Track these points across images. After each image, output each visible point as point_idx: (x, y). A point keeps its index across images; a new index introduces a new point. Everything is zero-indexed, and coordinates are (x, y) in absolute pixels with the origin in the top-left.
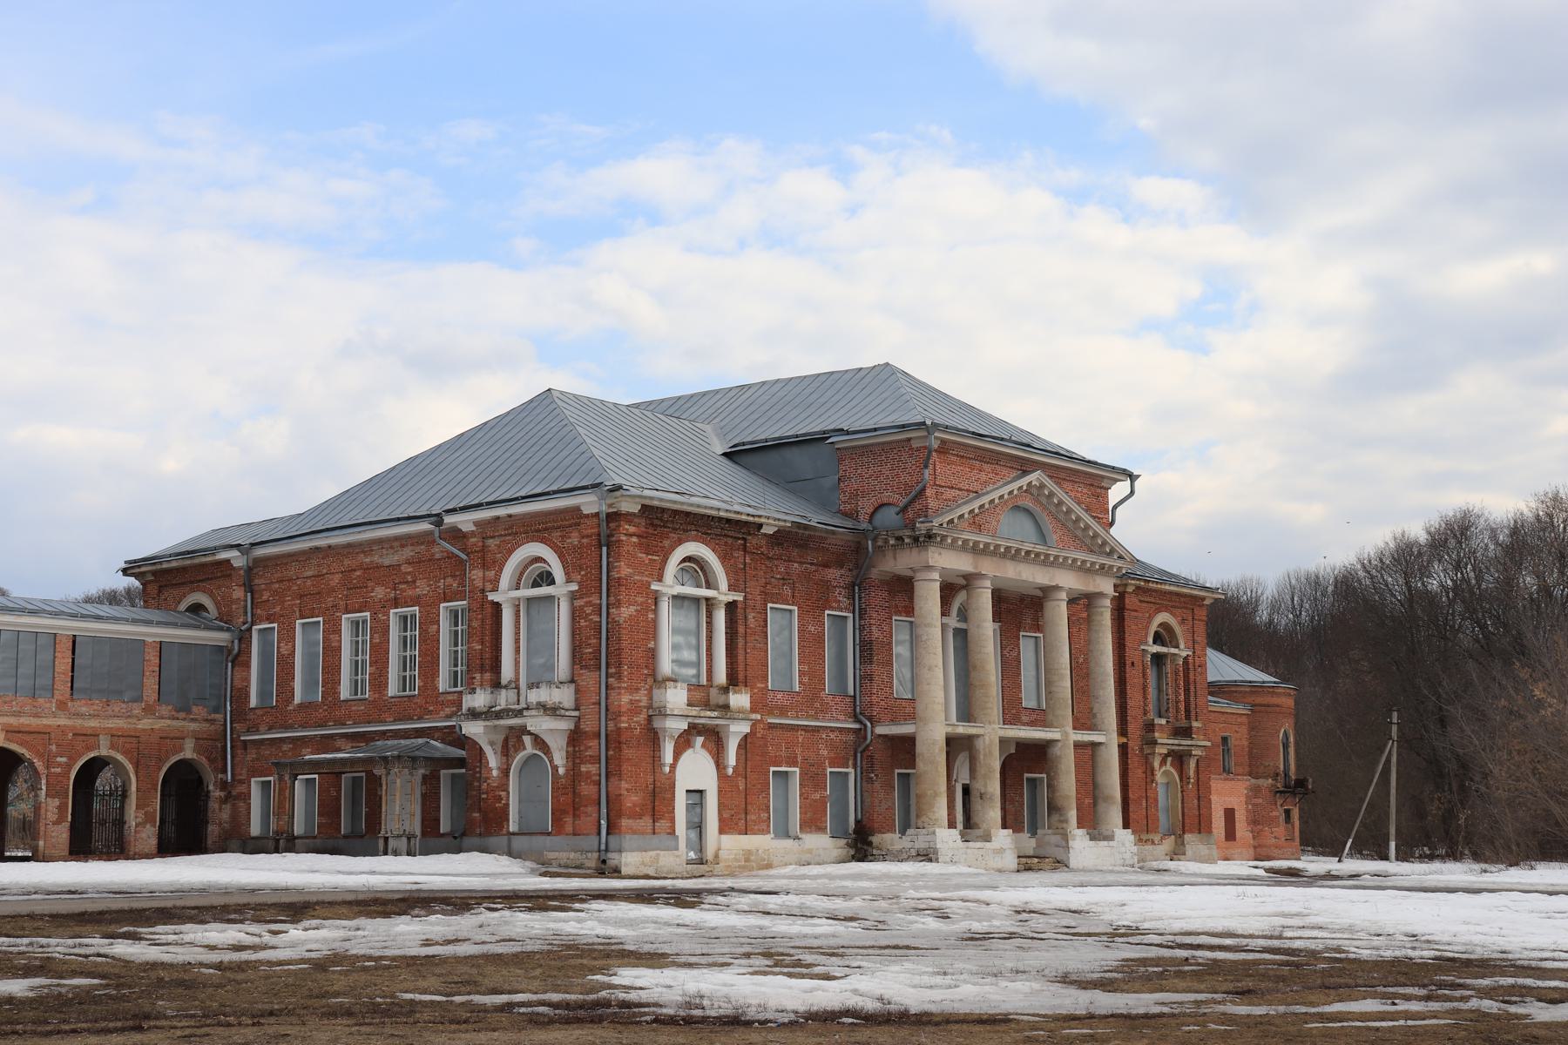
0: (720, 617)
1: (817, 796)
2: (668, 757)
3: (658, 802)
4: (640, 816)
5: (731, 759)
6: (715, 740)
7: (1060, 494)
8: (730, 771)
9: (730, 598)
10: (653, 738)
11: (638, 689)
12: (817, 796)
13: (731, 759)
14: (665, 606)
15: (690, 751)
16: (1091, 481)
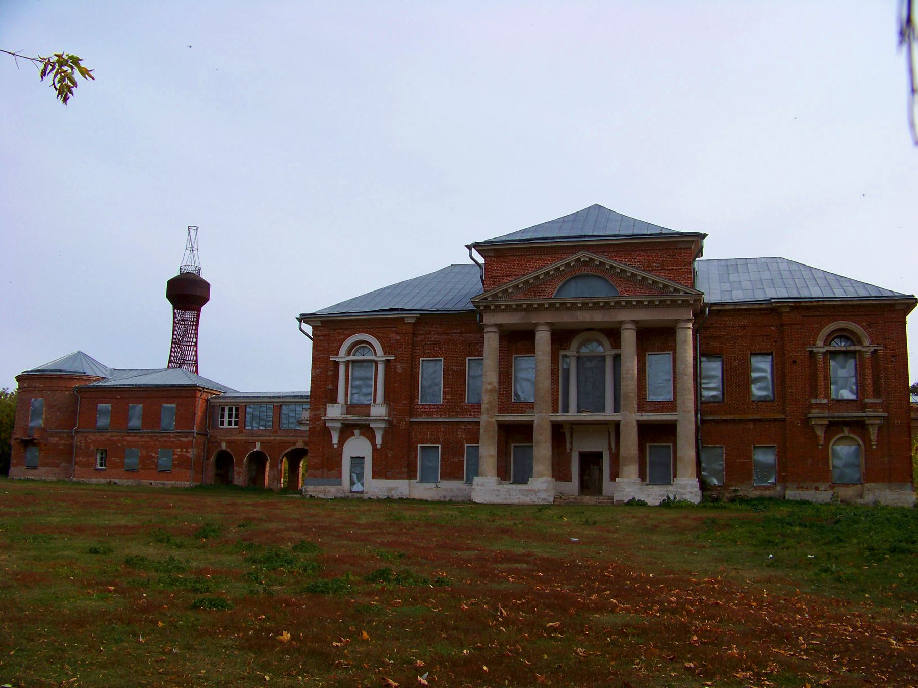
0: (381, 368)
1: (456, 460)
2: (335, 440)
3: (330, 464)
4: (319, 469)
5: (379, 440)
6: (367, 431)
7: (609, 262)
8: (379, 447)
9: (384, 359)
10: (327, 432)
11: (319, 409)
12: (456, 460)
13: (379, 440)
14: (342, 369)
15: (353, 438)
16: (688, 245)
